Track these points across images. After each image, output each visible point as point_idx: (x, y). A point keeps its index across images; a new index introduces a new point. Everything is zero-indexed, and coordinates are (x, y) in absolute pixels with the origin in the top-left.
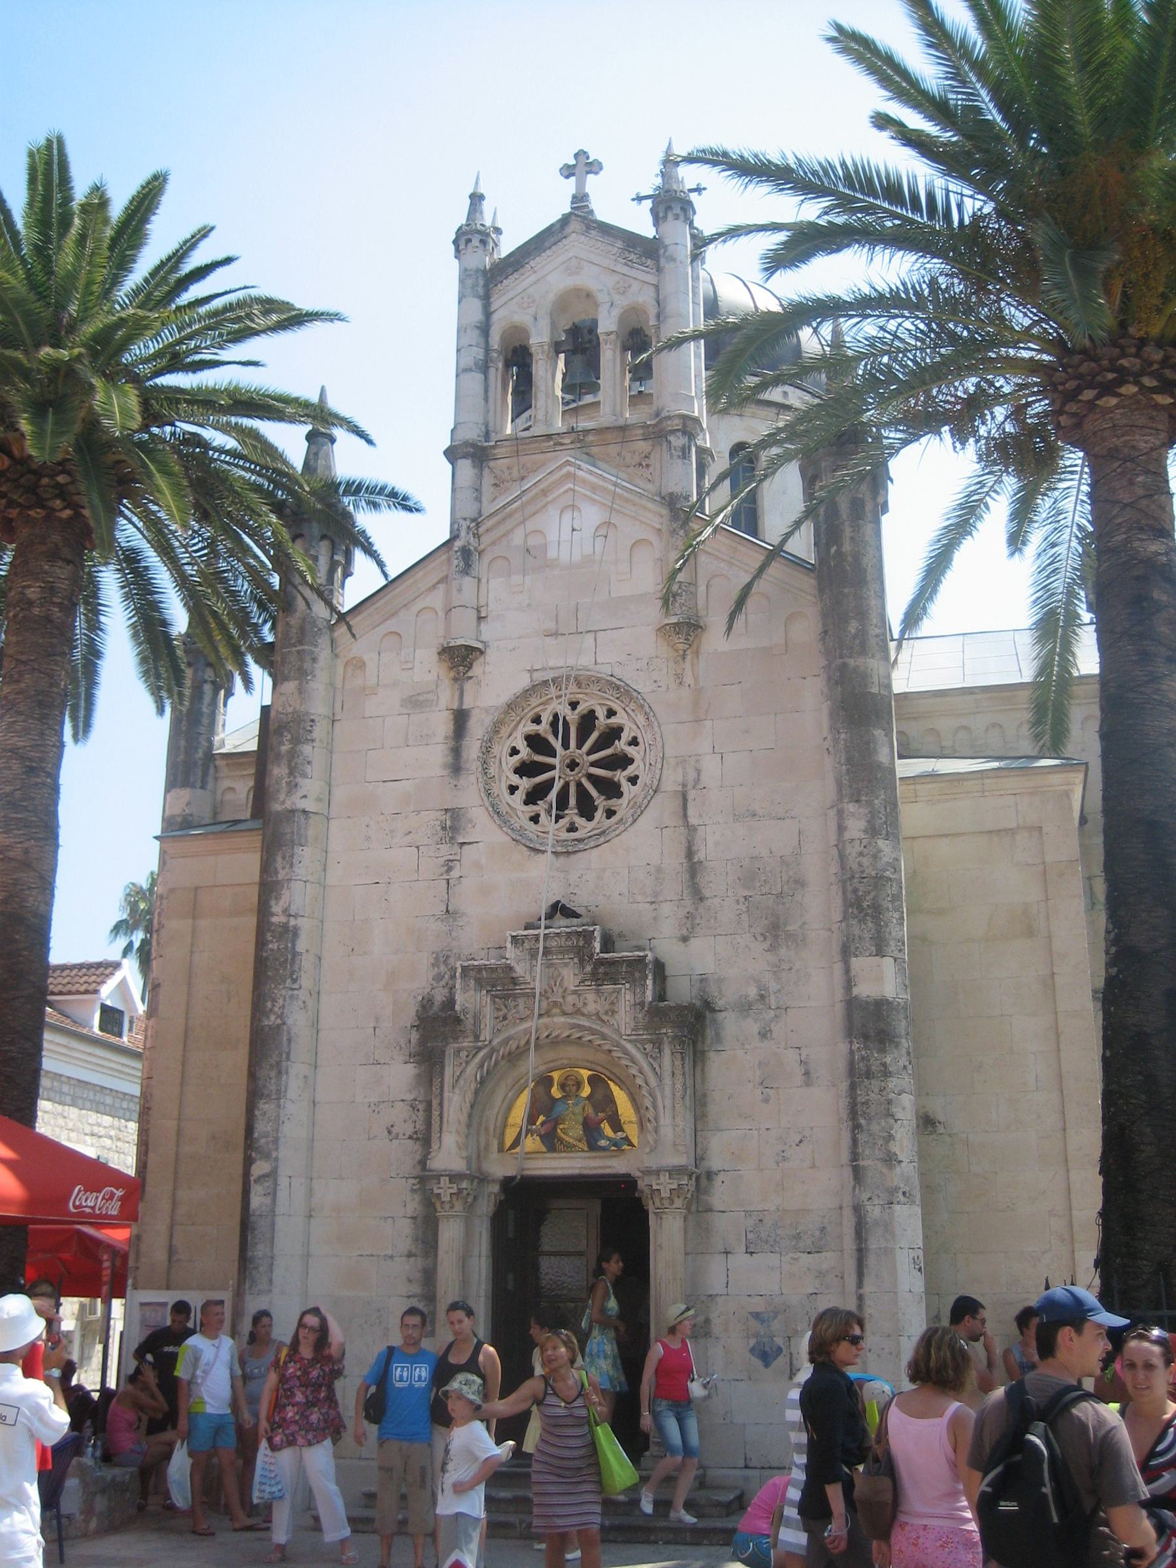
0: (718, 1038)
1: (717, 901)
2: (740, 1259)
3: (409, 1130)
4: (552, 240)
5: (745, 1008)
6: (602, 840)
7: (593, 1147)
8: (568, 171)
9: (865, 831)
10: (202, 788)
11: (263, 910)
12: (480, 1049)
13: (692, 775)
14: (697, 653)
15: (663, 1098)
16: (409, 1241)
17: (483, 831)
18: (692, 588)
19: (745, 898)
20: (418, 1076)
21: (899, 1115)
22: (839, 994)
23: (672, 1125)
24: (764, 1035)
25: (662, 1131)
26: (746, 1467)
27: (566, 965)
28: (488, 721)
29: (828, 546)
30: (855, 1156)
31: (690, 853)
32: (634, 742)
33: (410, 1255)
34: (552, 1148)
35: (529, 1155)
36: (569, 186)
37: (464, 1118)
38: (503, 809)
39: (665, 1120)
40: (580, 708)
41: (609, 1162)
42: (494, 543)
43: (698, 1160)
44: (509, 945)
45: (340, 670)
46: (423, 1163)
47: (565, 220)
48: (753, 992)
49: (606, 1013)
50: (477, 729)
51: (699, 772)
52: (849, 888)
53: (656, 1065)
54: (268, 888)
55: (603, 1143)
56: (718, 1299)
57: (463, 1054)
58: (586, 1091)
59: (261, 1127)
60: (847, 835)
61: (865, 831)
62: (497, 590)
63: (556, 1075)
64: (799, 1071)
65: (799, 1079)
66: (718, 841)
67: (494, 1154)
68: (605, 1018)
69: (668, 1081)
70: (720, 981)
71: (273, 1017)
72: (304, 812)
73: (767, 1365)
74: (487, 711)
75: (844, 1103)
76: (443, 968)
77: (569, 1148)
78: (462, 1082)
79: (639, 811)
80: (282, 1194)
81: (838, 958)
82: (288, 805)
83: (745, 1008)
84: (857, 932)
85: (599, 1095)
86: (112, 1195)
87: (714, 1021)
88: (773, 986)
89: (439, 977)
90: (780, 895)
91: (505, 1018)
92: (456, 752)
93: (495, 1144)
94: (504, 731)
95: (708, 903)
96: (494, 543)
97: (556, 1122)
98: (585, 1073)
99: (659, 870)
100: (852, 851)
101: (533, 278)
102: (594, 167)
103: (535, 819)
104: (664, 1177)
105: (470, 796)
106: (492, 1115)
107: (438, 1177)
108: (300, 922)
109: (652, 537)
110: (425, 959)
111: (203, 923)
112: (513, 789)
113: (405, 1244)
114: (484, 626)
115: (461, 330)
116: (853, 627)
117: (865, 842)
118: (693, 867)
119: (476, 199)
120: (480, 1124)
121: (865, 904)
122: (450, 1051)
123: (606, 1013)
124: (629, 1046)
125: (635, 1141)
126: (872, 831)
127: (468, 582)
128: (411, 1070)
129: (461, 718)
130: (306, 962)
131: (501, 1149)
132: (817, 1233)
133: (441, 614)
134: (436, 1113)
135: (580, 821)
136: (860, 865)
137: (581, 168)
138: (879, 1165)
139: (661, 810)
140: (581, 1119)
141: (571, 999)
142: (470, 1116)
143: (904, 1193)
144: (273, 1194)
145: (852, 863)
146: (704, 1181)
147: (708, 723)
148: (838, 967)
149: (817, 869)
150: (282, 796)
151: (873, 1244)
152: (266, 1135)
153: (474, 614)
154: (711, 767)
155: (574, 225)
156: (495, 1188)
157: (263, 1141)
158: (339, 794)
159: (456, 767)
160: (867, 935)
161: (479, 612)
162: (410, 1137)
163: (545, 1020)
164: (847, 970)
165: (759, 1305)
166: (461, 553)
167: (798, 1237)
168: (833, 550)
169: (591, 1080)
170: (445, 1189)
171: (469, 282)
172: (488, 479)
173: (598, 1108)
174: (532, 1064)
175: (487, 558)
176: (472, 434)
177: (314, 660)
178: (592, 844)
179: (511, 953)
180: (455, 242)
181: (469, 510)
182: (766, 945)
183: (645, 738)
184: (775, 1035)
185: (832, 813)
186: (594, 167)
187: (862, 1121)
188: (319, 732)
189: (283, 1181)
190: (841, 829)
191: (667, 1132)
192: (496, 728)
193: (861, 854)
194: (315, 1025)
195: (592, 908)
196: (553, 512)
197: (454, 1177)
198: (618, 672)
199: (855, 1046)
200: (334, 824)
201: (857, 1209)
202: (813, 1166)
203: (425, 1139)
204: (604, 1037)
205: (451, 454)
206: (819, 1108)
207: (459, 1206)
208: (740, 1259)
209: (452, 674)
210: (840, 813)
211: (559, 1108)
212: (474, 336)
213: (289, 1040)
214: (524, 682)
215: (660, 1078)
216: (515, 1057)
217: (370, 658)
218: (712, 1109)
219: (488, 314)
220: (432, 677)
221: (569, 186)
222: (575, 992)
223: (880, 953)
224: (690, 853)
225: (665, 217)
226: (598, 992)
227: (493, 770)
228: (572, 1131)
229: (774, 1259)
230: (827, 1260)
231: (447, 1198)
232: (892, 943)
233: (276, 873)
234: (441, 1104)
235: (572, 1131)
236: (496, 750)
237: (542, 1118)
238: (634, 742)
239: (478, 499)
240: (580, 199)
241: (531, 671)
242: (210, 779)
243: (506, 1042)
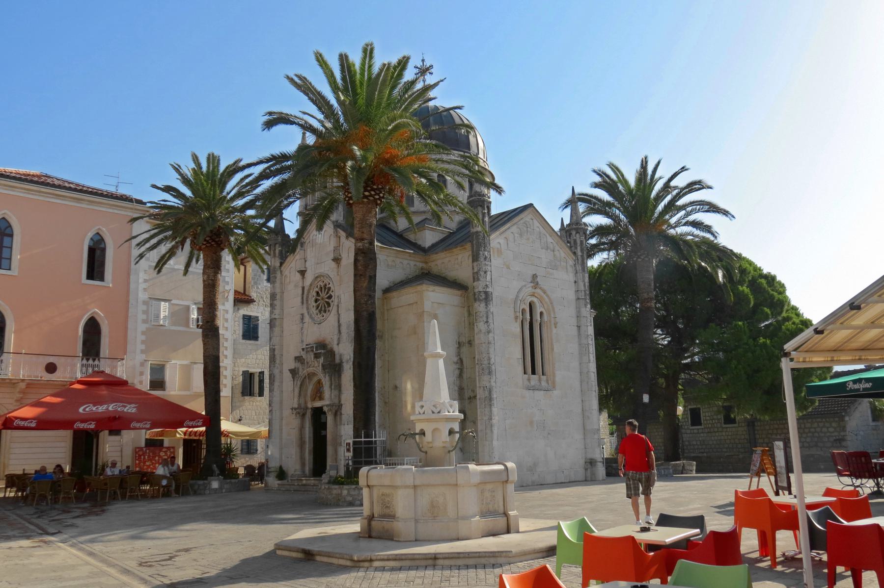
17: (307, 319)
118: (339, 326)
139: (335, 308)
154: (342, 297)
159: (303, 303)
194: (281, 372)
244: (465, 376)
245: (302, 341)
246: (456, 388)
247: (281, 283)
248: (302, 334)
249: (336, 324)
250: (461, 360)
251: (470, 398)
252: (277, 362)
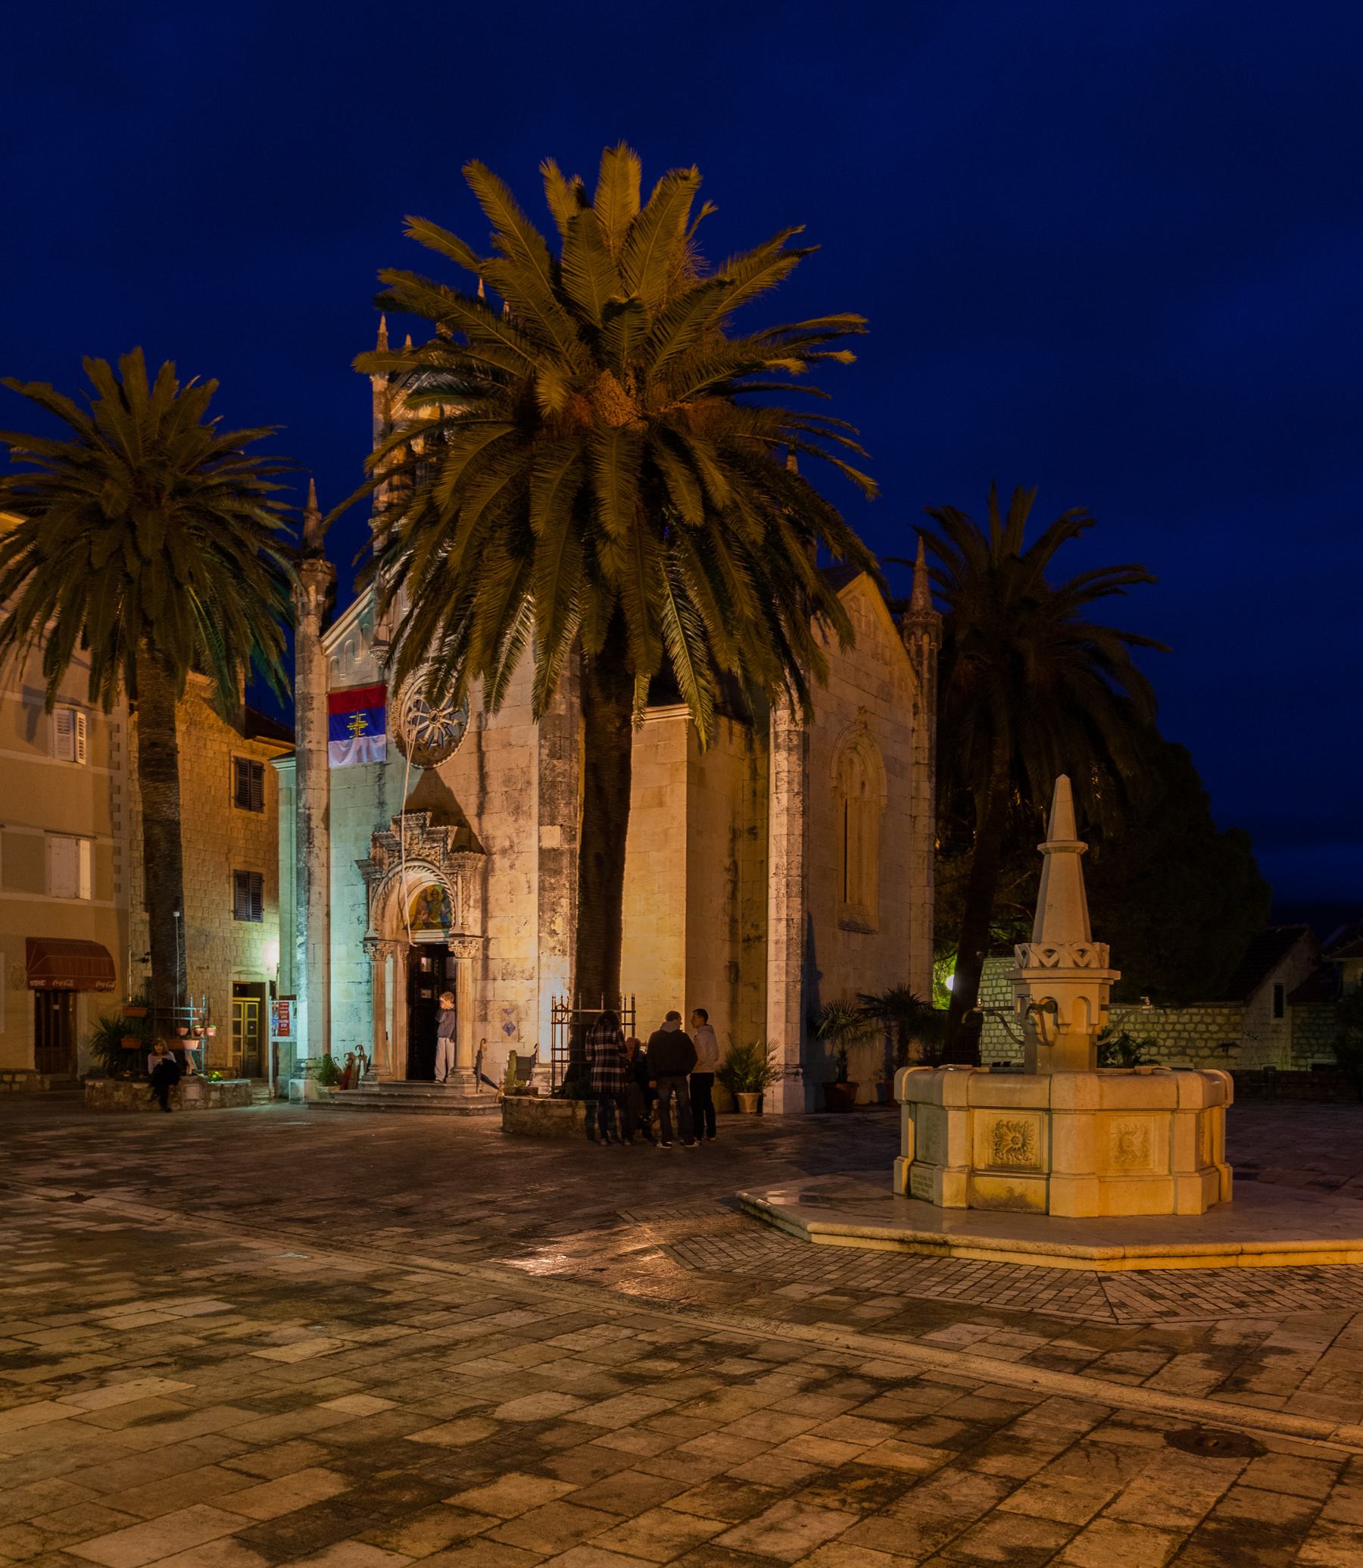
2: (499, 982)
5: (504, 852)
21: (559, 909)
31: (481, 766)
48: (507, 844)
83: (504, 852)
88: (516, 841)
165: (506, 1005)
223: (553, 824)
224: (481, 766)
244: (739, 896)
245: (382, 804)
246: (727, 919)
248: (381, 788)
249: (475, 774)
250: (735, 863)
251: (747, 940)
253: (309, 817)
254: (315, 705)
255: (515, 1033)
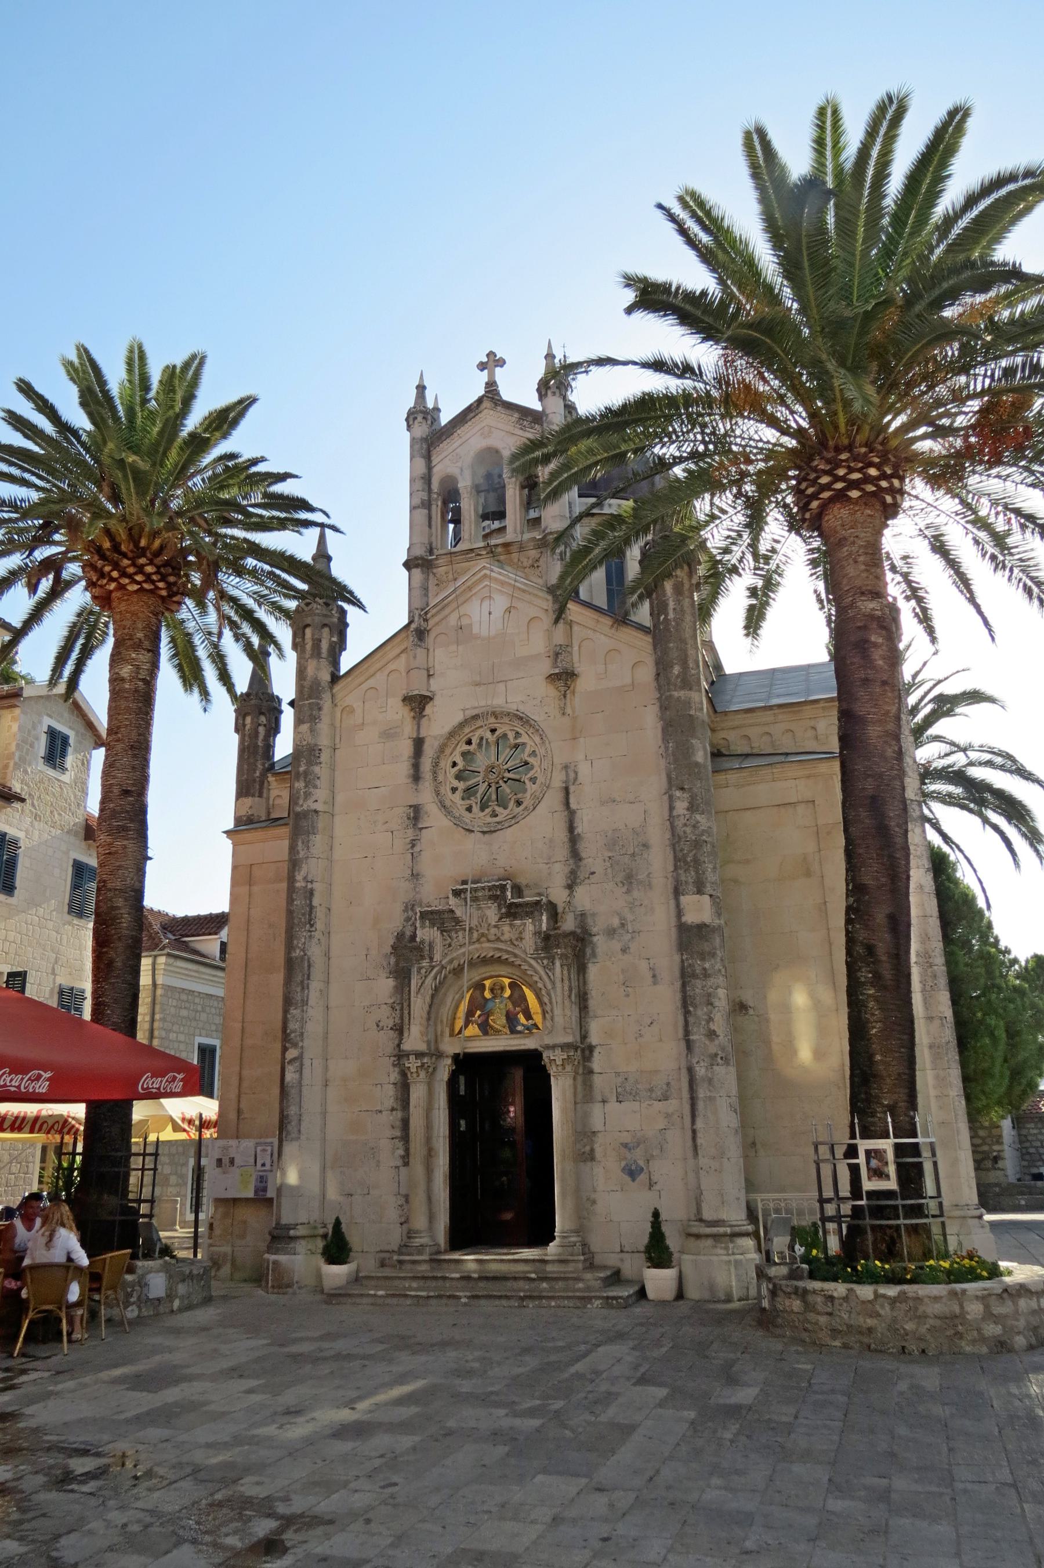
0: (594, 955)
1: (590, 860)
2: (613, 1106)
3: (391, 1023)
4: (472, 415)
5: (611, 932)
6: (513, 822)
7: (513, 1031)
8: (482, 366)
9: (688, 809)
10: (260, 796)
11: (291, 879)
12: (433, 967)
13: (572, 775)
14: (573, 693)
15: (556, 996)
16: (392, 1100)
17: (435, 818)
18: (569, 649)
19: (610, 858)
20: (396, 987)
21: (717, 1004)
22: (673, 921)
23: (564, 1013)
24: (624, 950)
25: (556, 1019)
26: (622, 1251)
27: (490, 908)
28: (436, 744)
29: (659, 615)
30: (687, 1032)
31: (571, 828)
32: (533, 753)
33: (393, 1109)
34: (485, 1033)
35: (469, 1038)
36: (484, 376)
37: (425, 1015)
38: (448, 803)
39: (558, 1011)
40: (497, 733)
41: (522, 1041)
42: (437, 624)
43: (584, 1037)
44: (451, 896)
45: (338, 715)
46: (399, 1045)
47: (480, 401)
48: (616, 922)
49: (517, 939)
50: (429, 750)
51: (576, 773)
52: (678, 849)
53: (550, 974)
54: (294, 864)
55: (519, 1028)
56: (600, 1135)
57: (423, 971)
58: (507, 993)
59: (292, 1026)
60: (675, 813)
61: (688, 809)
62: (442, 655)
63: (487, 983)
64: (648, 975)
65: (650, 980)
66: (590, 821)
67: (447, 1038)
68: (516, 943)
69: (559, 985)
70: (594, 915)
71: (298, 951)
72: (316, 812)
73: (633, 1180)
74: (435, 738)
75: (679, 996)
76: (410, 913)
77: (497, 1032)
78: (422, 990)
79: (538, 801)
80: (306, 1071)
81: (671, 896)
82: (305, 807)
83: (611, 932)
84: (683, 878)
85: (516, 995)
86: (175, 1078)
87: (591, 942)
88: (629, 917)
89: (408, 919)
90: (633, 855)
91: (450, 945)
92: (416, 766)
93: (447, 1031)
94: (448, 751)
95: (584, 862)
96: (437, 624)
97: (487, 1015)
98: (507, 981)
99: (551, 841)
100: (679, 823)
101: (459, 442)
102: (501, 363)
103: (469, 809)
104: (558, 1051)
105: (426, 796)
106: (445, 1012)
107: (408, 1055)
108: (315, 886)
109: (541, 614)
110: (399, 908)
111: (256, 889)
112: (454, 790)
113: (390, 1102)
114: (432, 681)
115: (412, 480)
116: (676, 670)
117: (687, 817)
118: (574, 839)
119: (421, 389)
120: (436, 1018)
121: (689, 859)
122: (414, 970)
123: (517, 939)
124: (533, 962)
125: (540, 1026)
126: (692, 808)
127: (420, 652)
128: (391, 982)
129: (419, 744)
130: (320, 913)
131: (452, 1035)
132: (665, 1087)
133: (404, 674)
134: (406, 1012)
135: (499, 810)
136: (685, 832)
137: (491, 363)
138: (703, 1038)
139: (553, 800)
140: (504, 1013)
141: (493, 931)
142: (429, 1013)
143: (722, 1058)
144: (300, 1071)
145: (680, 830)
146: (587, 1052)
147: (582, 740)
148: (672, 902)
149: (657, 836)
150: (301, 802)
151: (702, 1093)
152: (295, 1031)
153: (425, 672)
155: (486, 404)
156: (449, 1061)
157: (293, 1035)
158: (339, 798)
159: (416, 777)
160: (690, 880)
161: (428, 671)
162: (391, 1029)
163: (477, 946)
164: (678, 905)
165: (626, 1138)
166: (417, 631)
167: (651, 1090)
168: (662, 618)
169: (511, 985)
170: (413, 1064)
171: (417, 447)
172: (432, 581)
173: (515, 1004)
174: (470, 976)
175: (433, 634)
176: (419, 552)
177: (320, 709)
178: (507, 825)
179: (453, 901)
180: (407, 420)
181: (418, 604)
182: (624, 889)
183: (540, 751)
184: (632, 950)
185: (666, 797)
186: (501, 363)
187: (691, 1009)
188: (324, 757)
189: (307, 1062)
190: (671, 808)
191: (559, 1020)
192: (442, 749)
193: (685, 825)
194: (327, 955)
195: (508, 868)
196: (475, 603)
197: (419, 1055)
198: (521, 708)
199: (685, 957)
200: (337, 819)
201: (690, 1070)
202: (661, 1040)
203: (399, 1030)
204: (515, 956)
205: (407, 565)
206: (664, 999)
207: (422, 1074)
208: (613, 1106)
209: (412, 714)
210: (671, 799)
211: (490, 1005)
212: (419, 485)
213: (309, 966)
214: (459, 718)
215: (553, 983)
216: (458, 971)
217: (357, 705)
218: (592, 1003)
219: (430, 468)
220: (399, 717)
221: (484, 376)
222: (495, 926)
223: (700, 892)
224: (571, 828)
225: (546, 394)
226: (511, 925)
227: (441, 778)
228: (498, 1020)
229: (636, 1105)
230: (672, 1105)
231: (414, 1070)
232: (708, 885)
233: (298, 853)
234: (409, 1006)
235: (498, 1020)
236: (442, 764)
237: (479, 1012)
238: (533, 753)
239: (426, 595)
240: (491, 387)
241: (464, 710)
242: (265, 791)
243: (451, 961)
245: (415, 876)
247: (332, 725)
249: (562, 835)
252: (319, 925)
253: (311, 893)
254: (322, 759)
255: (643, 1177)
